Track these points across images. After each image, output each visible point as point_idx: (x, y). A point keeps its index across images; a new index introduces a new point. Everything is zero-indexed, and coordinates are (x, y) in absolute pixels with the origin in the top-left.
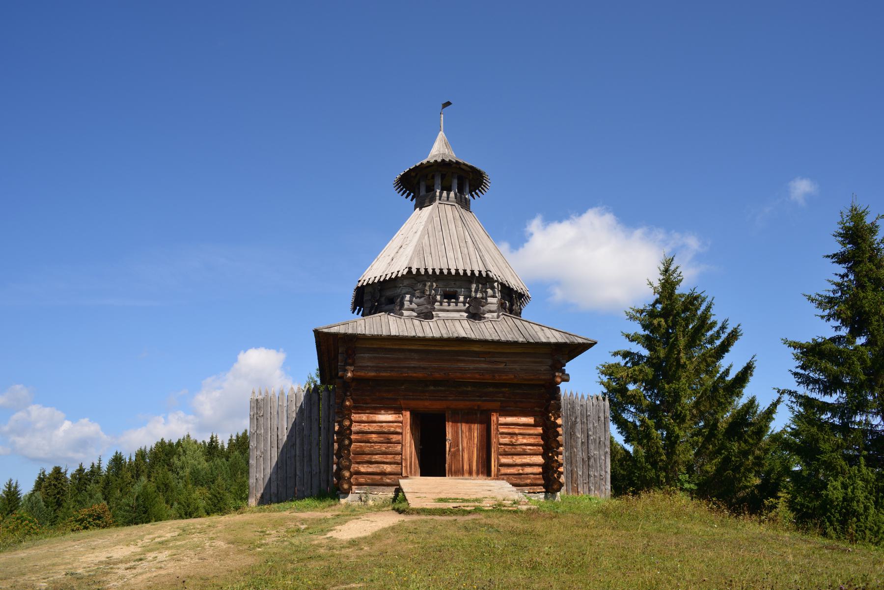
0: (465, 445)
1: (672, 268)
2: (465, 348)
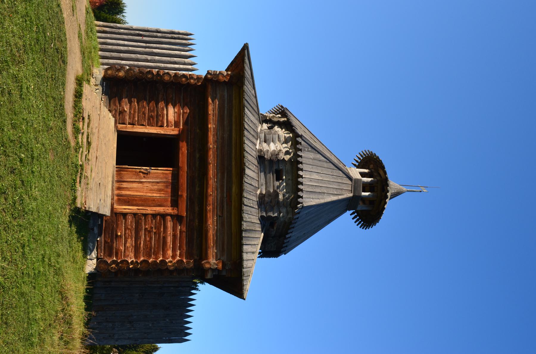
0: (146, 185)
2: (234, 179)
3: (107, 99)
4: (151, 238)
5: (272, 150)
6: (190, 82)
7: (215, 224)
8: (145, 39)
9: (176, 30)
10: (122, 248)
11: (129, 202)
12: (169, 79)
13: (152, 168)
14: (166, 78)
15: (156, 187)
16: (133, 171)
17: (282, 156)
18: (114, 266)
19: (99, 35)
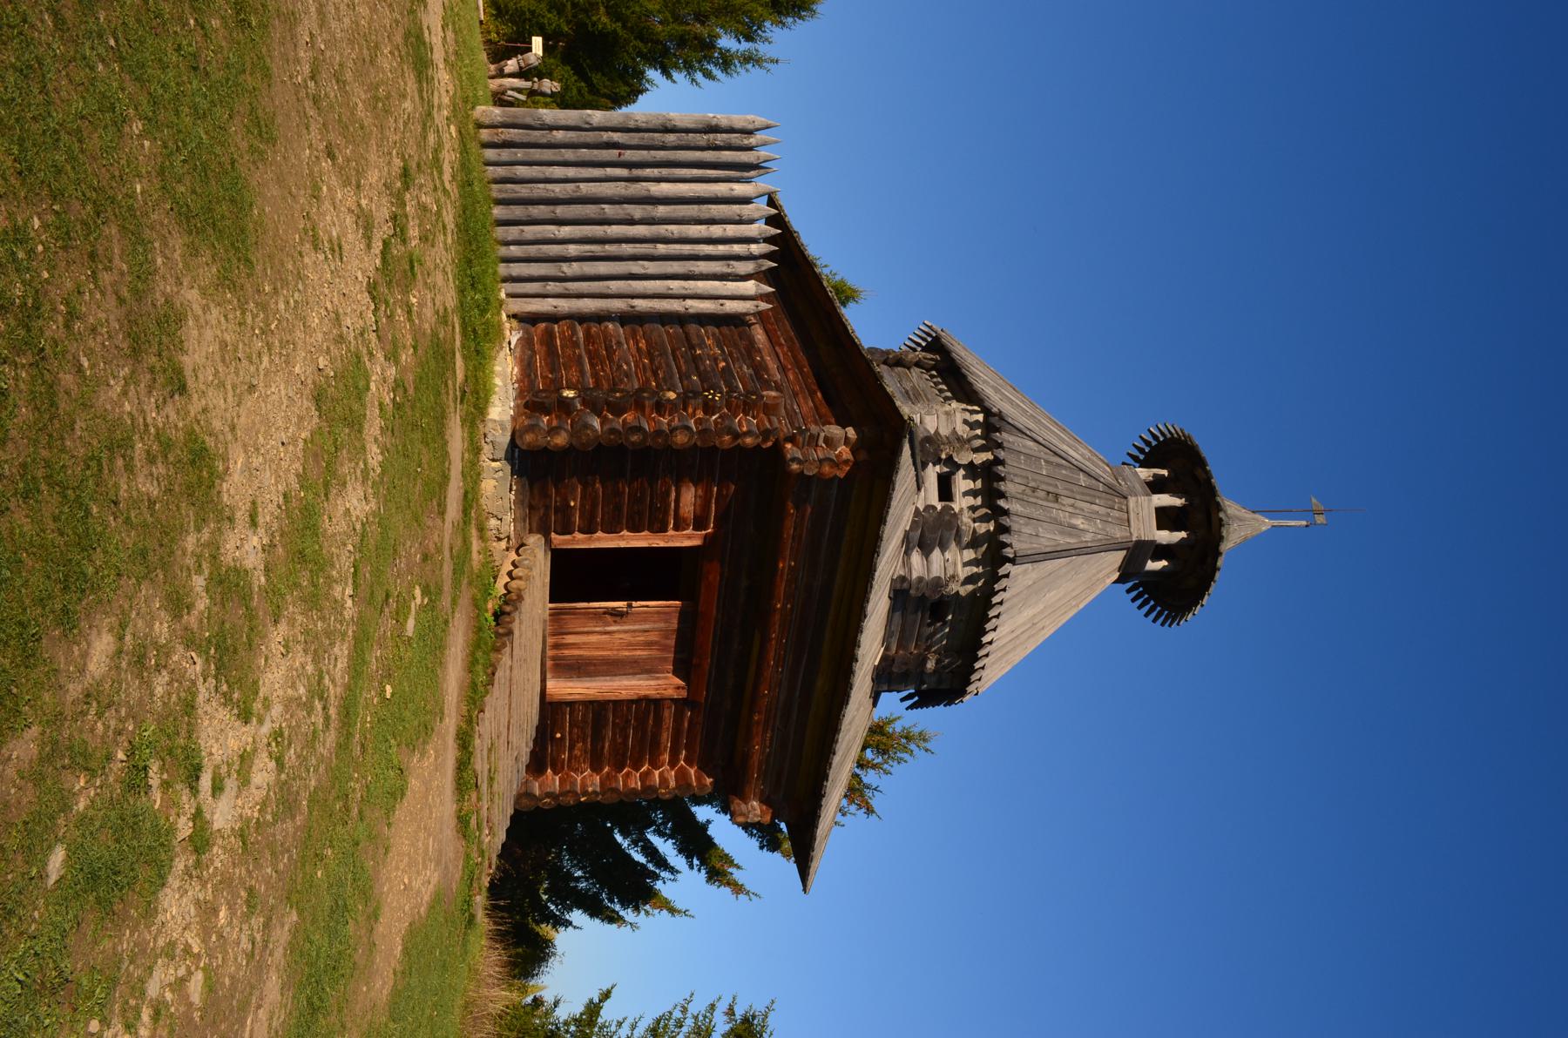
0: (617, 636)
1: (912, 746)
3: (523, 486)
4: (626, 738)
5: (932, 576)
6: (744, 442)
7: (768, 744)
8: (629, 155)
9: (723, 119)
10: (565, 756)
11: (579, 668)
12: (686, 440)
13: (634, 604)
14: (681, 439)
15: (642, 638)
16: (589, 613)
17: (954, 587)
18: (547, 800)
19: (490, 154)
